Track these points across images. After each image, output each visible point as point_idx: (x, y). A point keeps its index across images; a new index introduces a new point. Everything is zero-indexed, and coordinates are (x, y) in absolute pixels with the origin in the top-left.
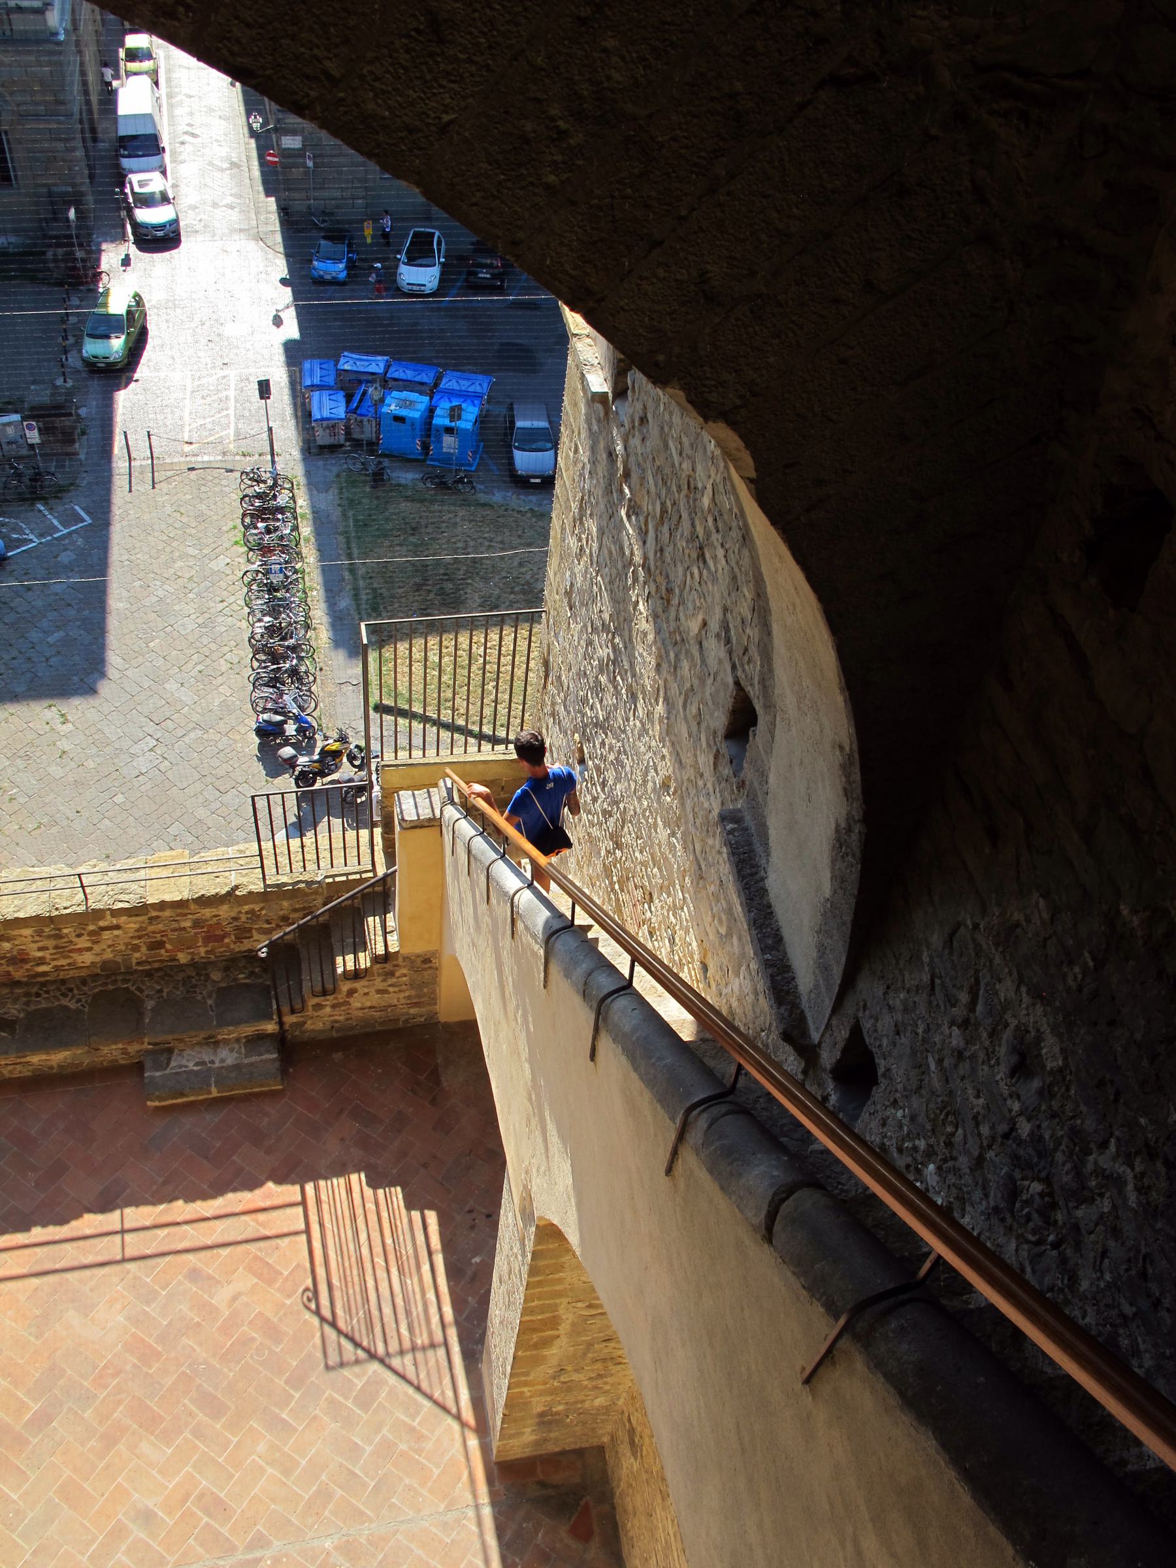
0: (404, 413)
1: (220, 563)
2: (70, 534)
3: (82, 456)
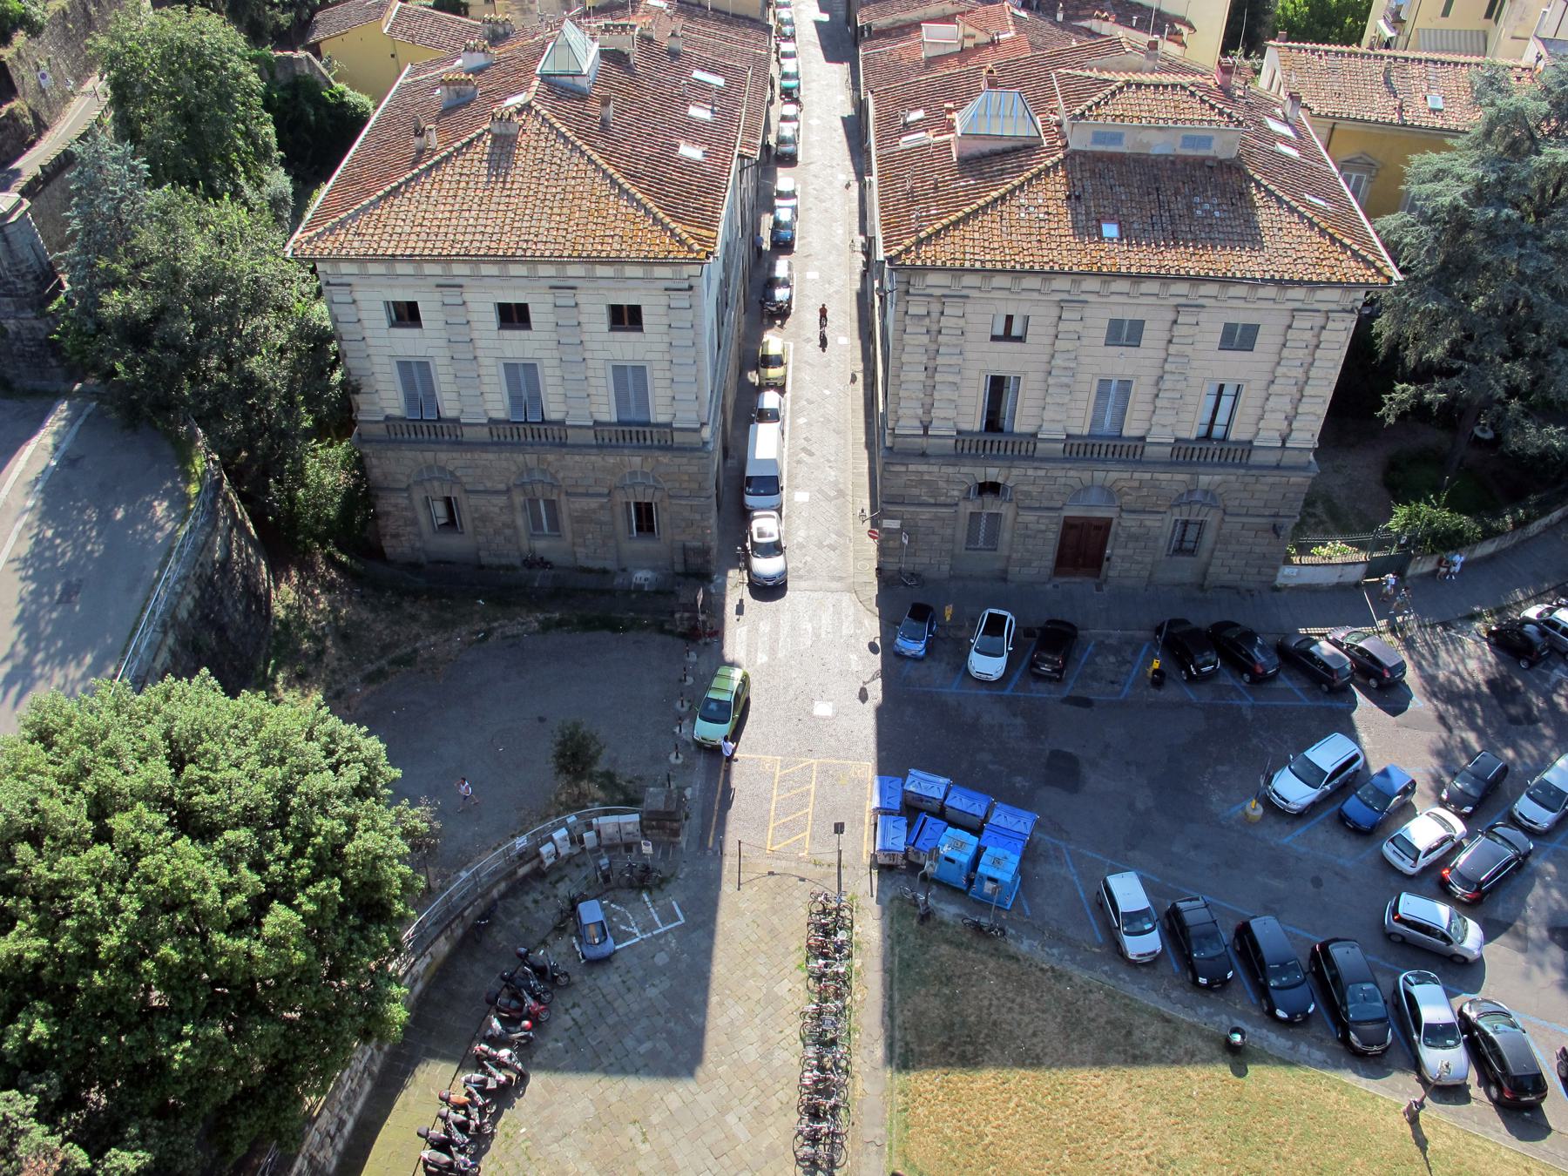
0: (955, 855)
1: (783, 988)
2: (666, 933)
3: (684, 845)
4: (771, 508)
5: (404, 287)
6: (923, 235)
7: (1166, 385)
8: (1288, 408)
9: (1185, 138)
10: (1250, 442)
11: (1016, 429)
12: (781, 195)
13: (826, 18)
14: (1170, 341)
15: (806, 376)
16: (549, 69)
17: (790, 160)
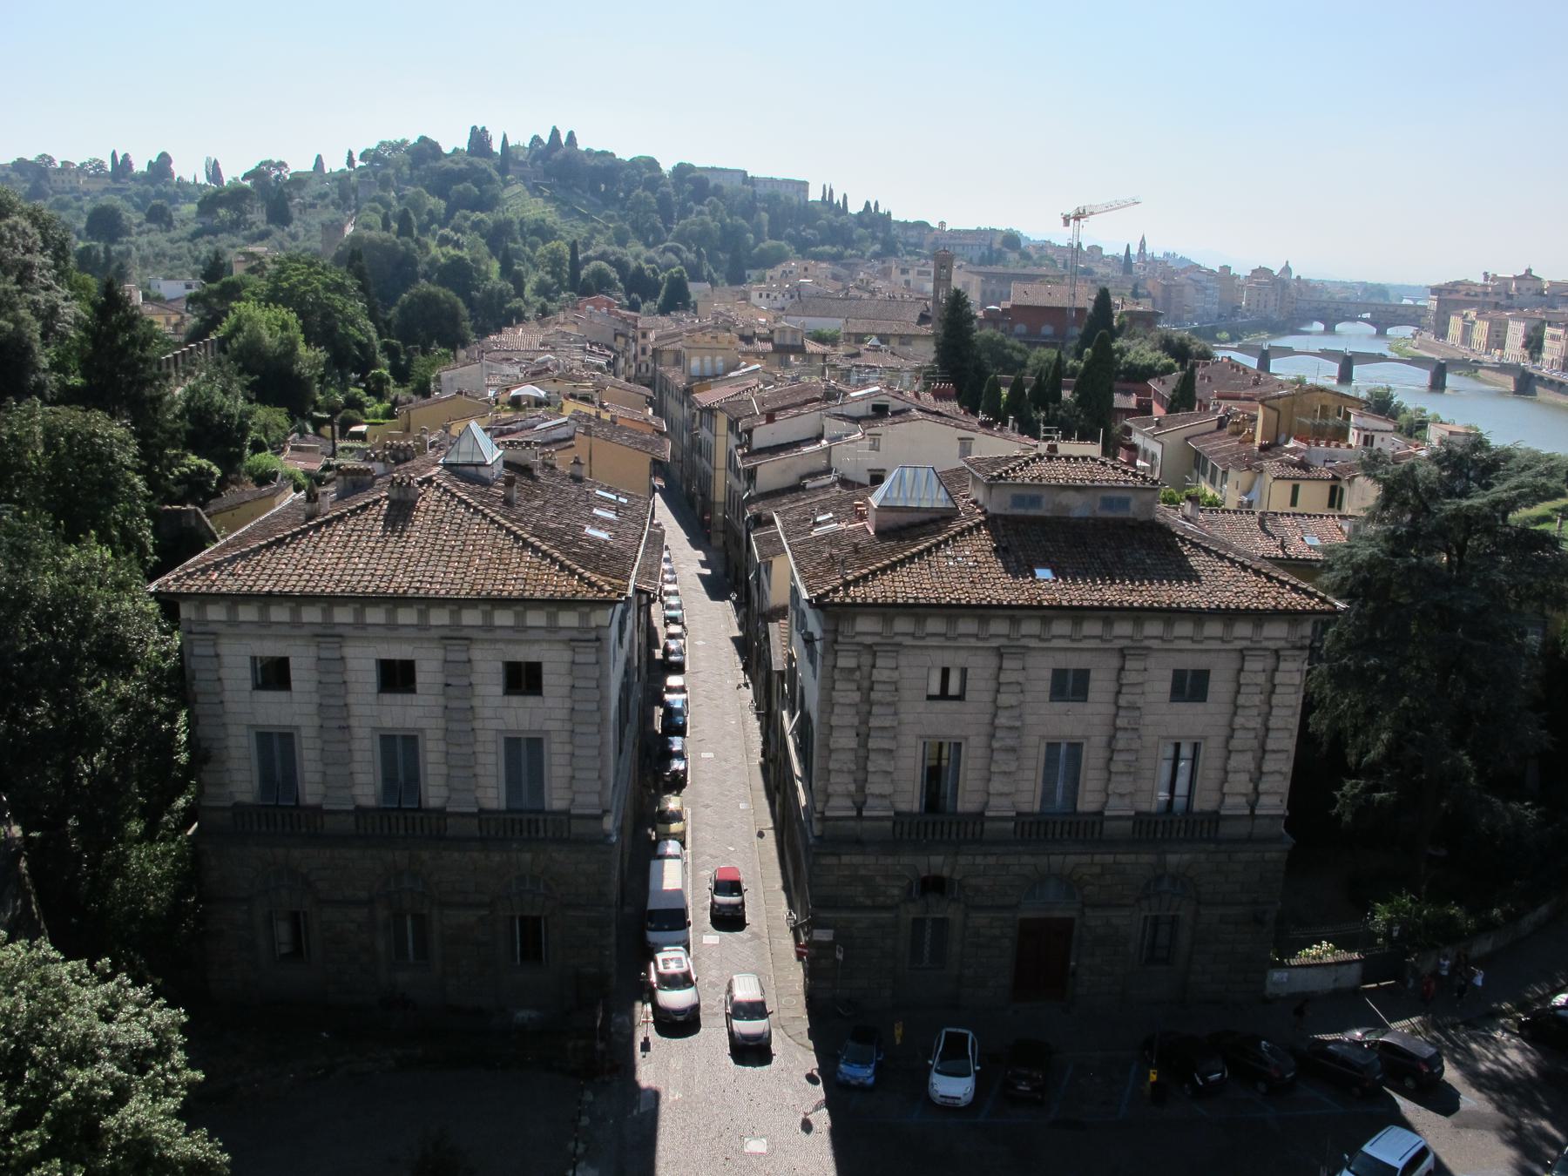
4: (677, 944)
5: (278, 637)
6: (849, 578)
7: (1121, 744)
8: (1252, 766)
9: (1104, 499)
10: (1216, 812)
11: (960, 808)
12: (671, 690)
13: (708, 572)
14: (1119, 693)
15: (706, 835)
16: (448, 460)
17: (679, 668)
